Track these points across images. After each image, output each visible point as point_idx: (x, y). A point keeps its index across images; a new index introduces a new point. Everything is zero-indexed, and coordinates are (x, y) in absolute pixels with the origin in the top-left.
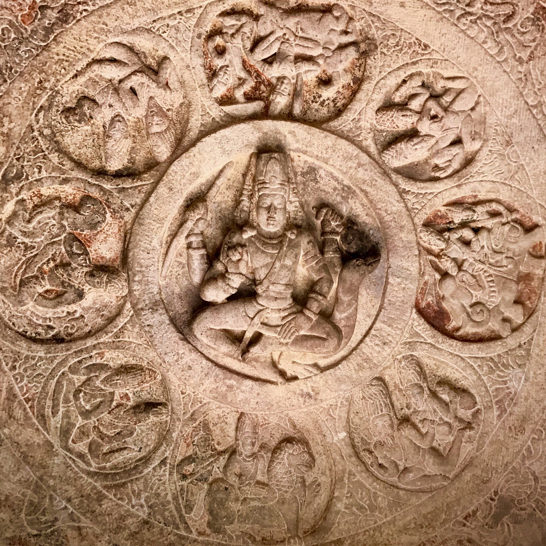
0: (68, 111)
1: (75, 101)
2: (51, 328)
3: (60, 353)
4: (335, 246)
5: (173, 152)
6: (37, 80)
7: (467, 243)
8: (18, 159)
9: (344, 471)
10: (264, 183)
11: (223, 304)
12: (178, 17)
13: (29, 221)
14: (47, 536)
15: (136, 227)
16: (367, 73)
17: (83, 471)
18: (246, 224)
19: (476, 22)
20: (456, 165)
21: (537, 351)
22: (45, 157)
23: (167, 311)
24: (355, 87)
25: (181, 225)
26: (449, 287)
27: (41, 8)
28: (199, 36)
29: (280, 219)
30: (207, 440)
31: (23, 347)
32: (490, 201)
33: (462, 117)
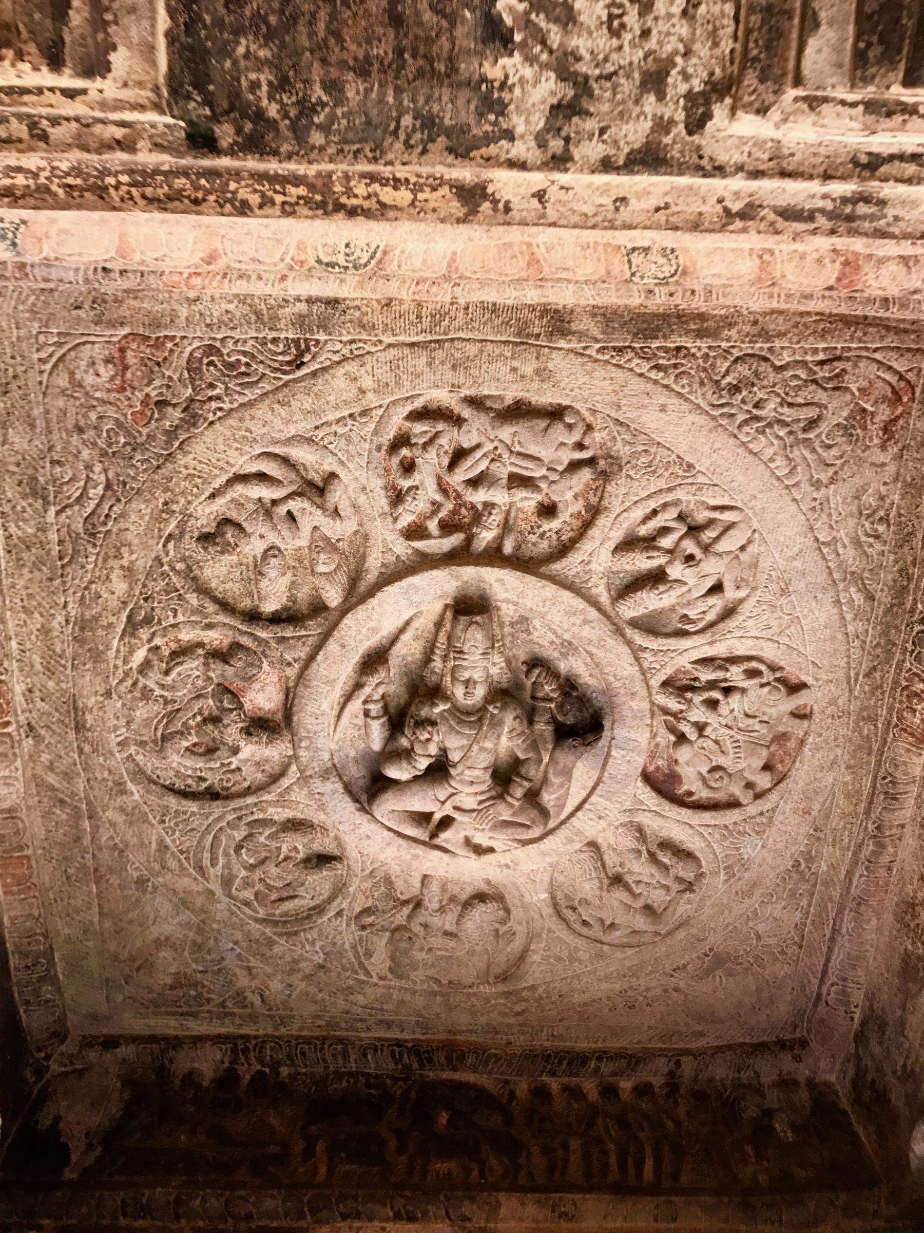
0: (205, 538)
1: (214, 524)
2: (203, 779)
3: (217, 809)
4: (547, 716)
5: (346, 599)
6: (162, 500)
7: (712, 704)
8: (146, 599)
9: (542, 928)
10: (461, 652)
11: (408, 782)
12: (350, 422)
13: (167, 673)
14: (214, 973)
15: (301, 688)
16: (605, 503)
17: (251, 917)
18: (436, 693)
19: (763, 432)
20: (711, 616)
21: (781, 818)
22: (180, 597)
23: (341, 778)
24: (587, 516)
25: (358, 686)
26: (684, 754)
27: (158, 403)
28: (379, 449)
29: (480, 692)
30: (390, 895)
31: (172, 802)
32: (750, 658)
33: (727, 559)
